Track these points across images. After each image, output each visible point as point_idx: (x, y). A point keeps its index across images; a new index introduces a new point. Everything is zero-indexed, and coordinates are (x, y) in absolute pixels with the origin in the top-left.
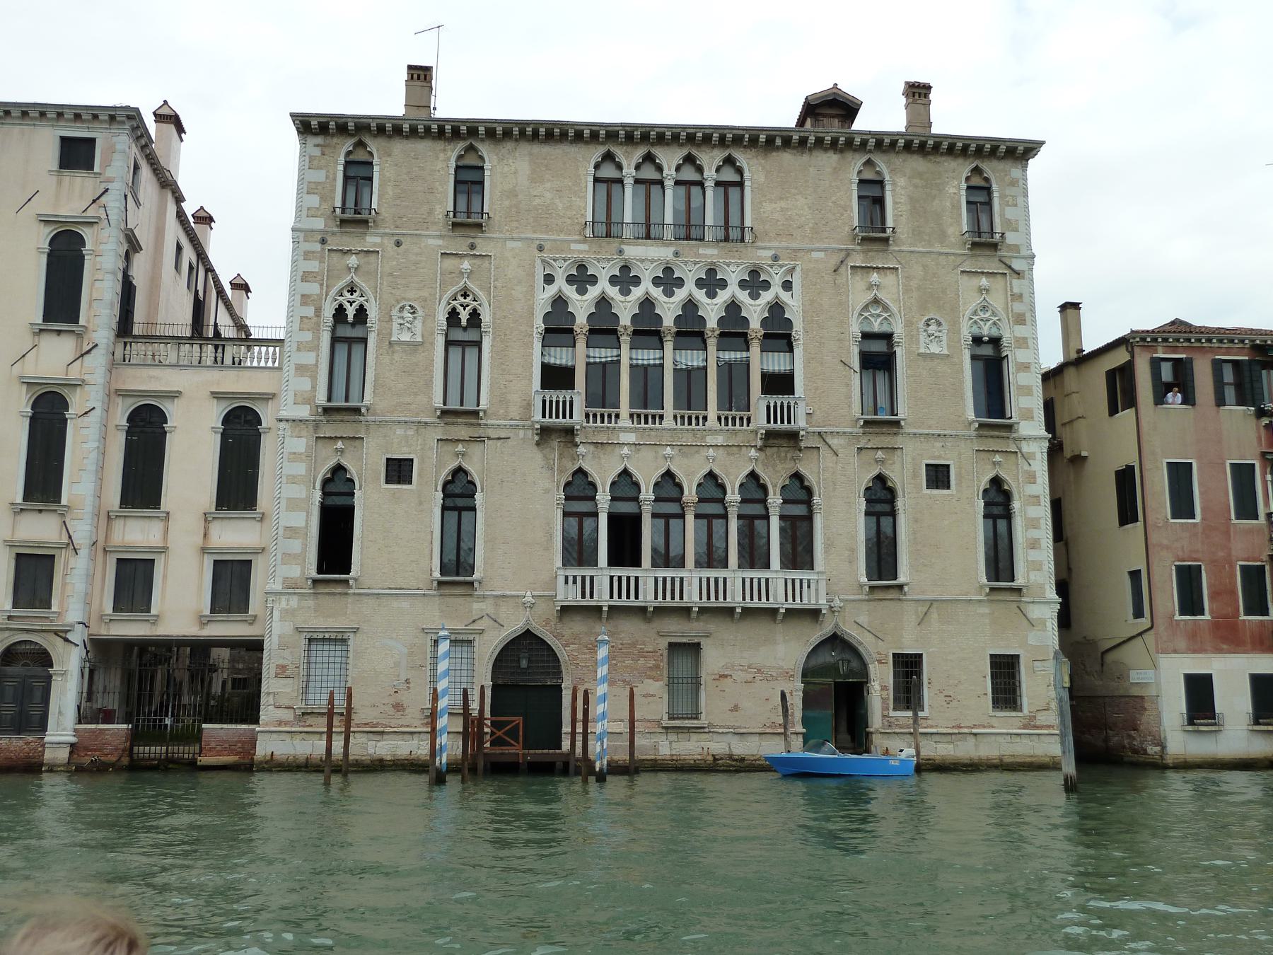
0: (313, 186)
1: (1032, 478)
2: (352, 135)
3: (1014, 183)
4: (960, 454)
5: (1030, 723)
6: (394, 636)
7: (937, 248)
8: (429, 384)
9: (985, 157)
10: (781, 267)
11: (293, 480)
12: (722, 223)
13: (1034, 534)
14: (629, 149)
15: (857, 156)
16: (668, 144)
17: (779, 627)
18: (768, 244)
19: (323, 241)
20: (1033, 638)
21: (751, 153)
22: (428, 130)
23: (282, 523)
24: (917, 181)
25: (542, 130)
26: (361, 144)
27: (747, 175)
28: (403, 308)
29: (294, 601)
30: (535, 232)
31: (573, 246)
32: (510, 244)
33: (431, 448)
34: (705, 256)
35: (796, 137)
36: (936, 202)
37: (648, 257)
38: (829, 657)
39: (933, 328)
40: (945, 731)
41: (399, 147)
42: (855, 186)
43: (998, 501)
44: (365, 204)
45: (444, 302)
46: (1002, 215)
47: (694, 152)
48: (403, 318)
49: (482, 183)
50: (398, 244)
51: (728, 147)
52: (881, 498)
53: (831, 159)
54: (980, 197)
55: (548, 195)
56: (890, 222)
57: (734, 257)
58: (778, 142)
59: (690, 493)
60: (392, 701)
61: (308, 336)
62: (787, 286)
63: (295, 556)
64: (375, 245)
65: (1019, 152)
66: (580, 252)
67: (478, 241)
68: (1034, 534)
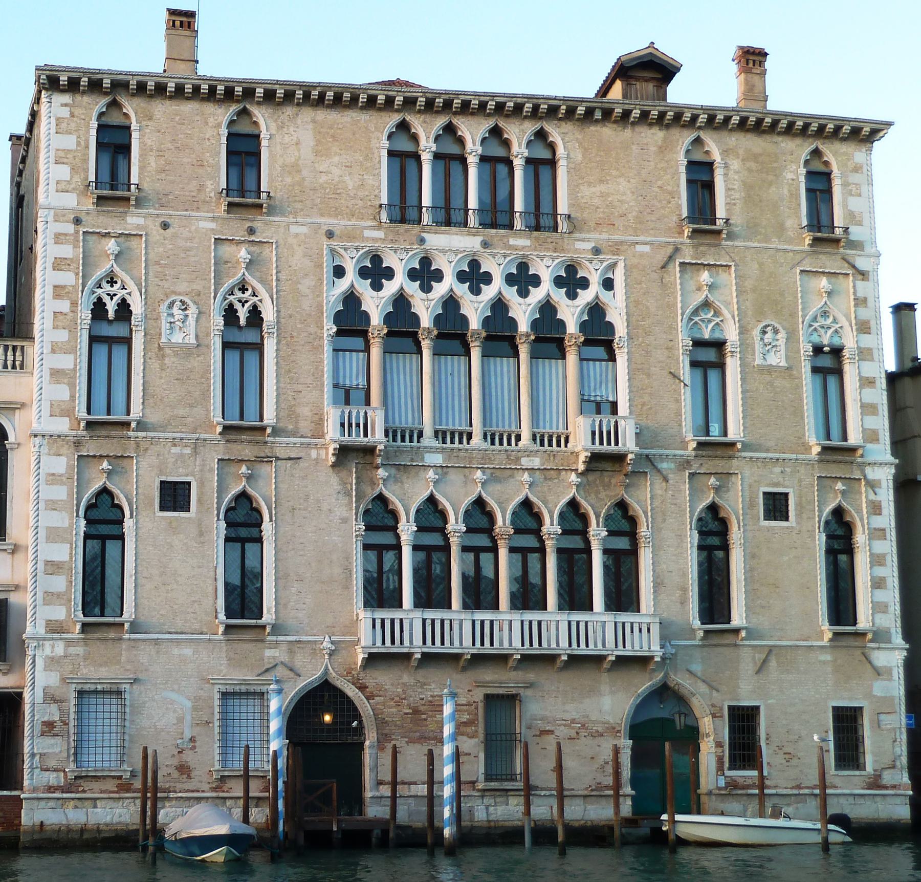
0: (62, 154)
1: (876, 509)
2: (106, 94)
3: (857, 169)
4: (800, 481)
5: (875, 783)
6: (176, 687)
7: (775, 244)
8: (205, 395)
9: (827, 137)
11: (52, 505)
12: (533, 210)
13: (880, 572)
14: (428, 117)
15: (686, 132)
16: (472, 114)
17: (605, 677)
18: (588, 236)
19: (77, 221)
20: (879, 688)
21: (567, 127)
22: (196, 89)
23: (41, 558)
24: (752, 165)
25: (330, 95)
26: (114, 104)
27: (561, 151)
28: (172, 304)
29: (60, 649)
30: (322, 215)
31: (367, 233)
32: (294, 229)
33: (211, 470)
34: (515, 248)
35: (618, 110)
36: (773, 189)
37: (450, 247)
38: (661, 711)
39: (769, 336)
40: (785, 792)
41: (162, 109)
42: (683, 169)
43: (840, 536)
44: (122, 178)
45: (219, 297)
46: (845, 205)
47: (501, 124)
49: (258, 155)
50: (165, 226)
51: (541, 118)
52: (714, 531)
53: (656, 135)
54: (820, 185)
55: (336, 171)
56: (721, 212)
57: (548, 250)
58: (598, 115)
59: (503, 522)
60: (175, 762)
61: (63, 336)
62: (608, 284)
63: (58, 595)
64: (138, 227)
65: (864, 134)
66: (375, 240)
67: (256, 225)
68: (880, 572)
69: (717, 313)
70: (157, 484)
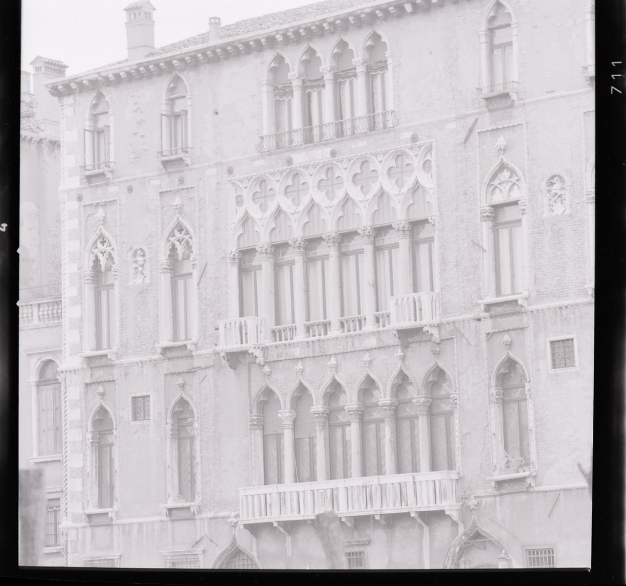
10: (420, 147)
19: (80, 198)
45: (163, 242)
48: (136, 262)
69: (513, 172)
70: (130, 400)
